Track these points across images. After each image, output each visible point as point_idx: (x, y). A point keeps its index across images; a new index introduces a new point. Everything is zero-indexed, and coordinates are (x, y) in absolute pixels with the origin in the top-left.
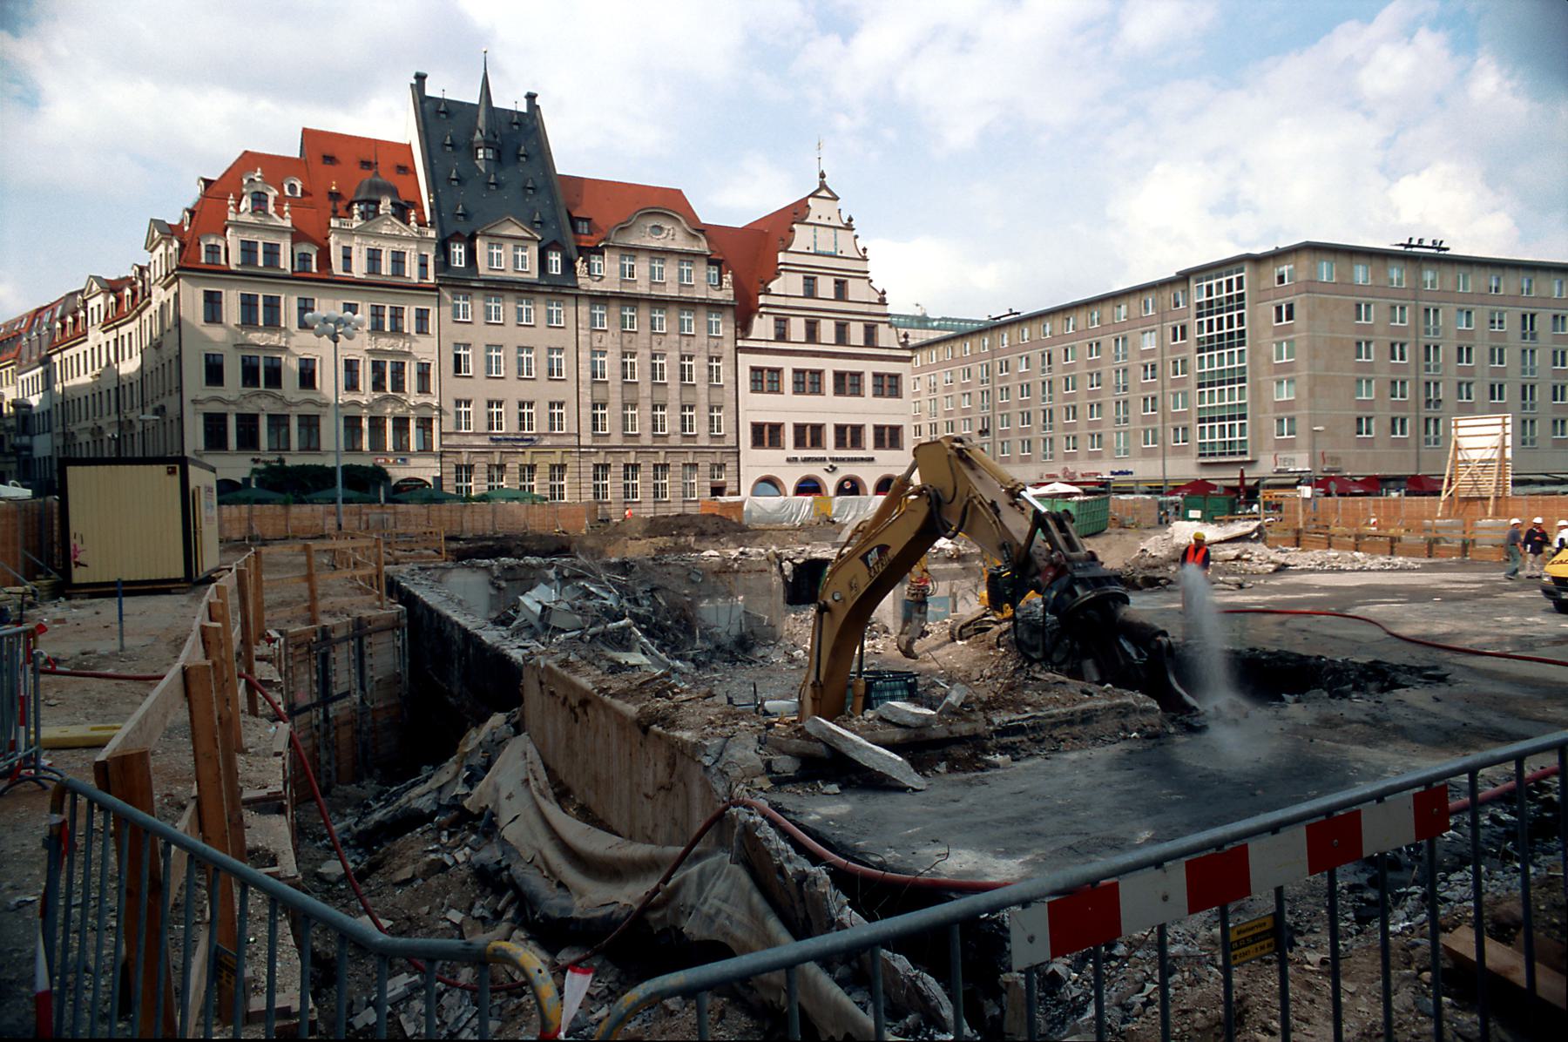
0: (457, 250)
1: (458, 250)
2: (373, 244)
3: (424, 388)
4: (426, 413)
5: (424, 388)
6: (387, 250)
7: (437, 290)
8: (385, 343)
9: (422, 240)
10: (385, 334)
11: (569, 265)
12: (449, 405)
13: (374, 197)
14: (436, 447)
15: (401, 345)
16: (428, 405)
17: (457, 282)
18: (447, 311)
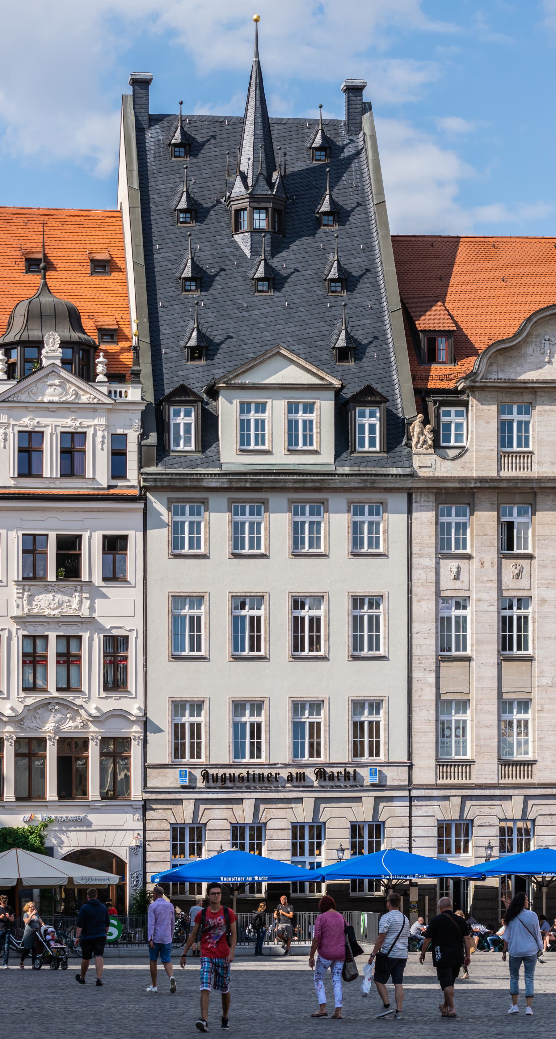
0: (182, 420)
1: (183, 420)
2: (28, 422)
3: (115, 682)
4: (117, 729)
5: (115, 682)
6: (52, 427)
7: (142, 498)
8: (46, 603)
9: (116, 405)
10: (47, 588)
11: (396, 432)
12: (161, 717)
13: (35, 334)
14: (136, 792)
15: (75, 604)
16: (121, 715)
17: (178, 479)
18: (160, 538)
